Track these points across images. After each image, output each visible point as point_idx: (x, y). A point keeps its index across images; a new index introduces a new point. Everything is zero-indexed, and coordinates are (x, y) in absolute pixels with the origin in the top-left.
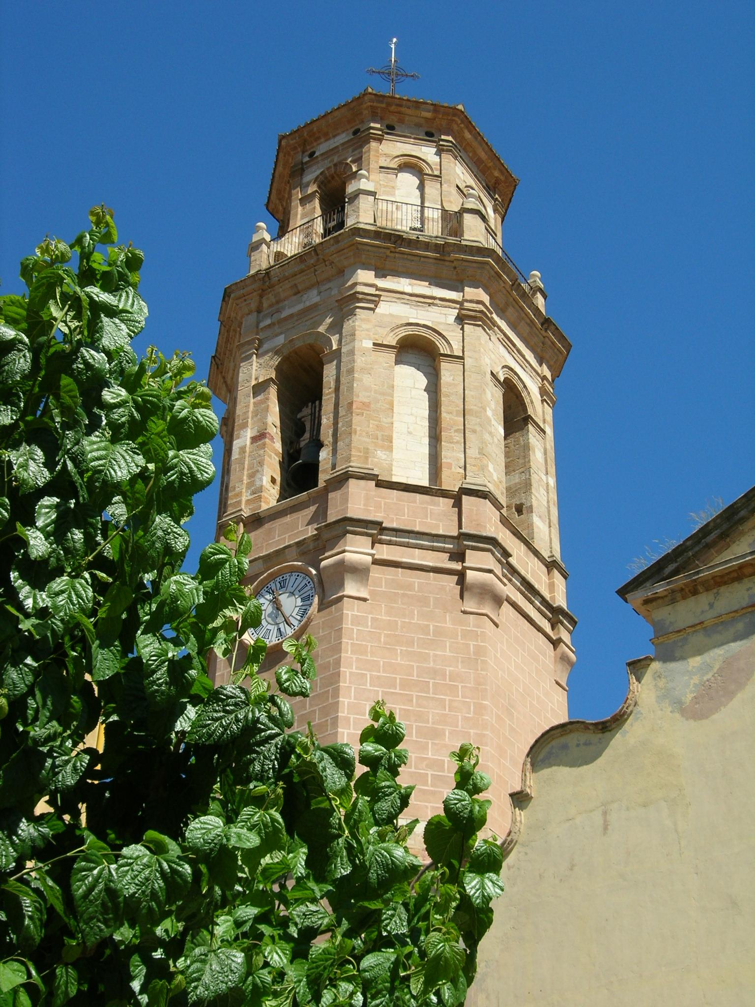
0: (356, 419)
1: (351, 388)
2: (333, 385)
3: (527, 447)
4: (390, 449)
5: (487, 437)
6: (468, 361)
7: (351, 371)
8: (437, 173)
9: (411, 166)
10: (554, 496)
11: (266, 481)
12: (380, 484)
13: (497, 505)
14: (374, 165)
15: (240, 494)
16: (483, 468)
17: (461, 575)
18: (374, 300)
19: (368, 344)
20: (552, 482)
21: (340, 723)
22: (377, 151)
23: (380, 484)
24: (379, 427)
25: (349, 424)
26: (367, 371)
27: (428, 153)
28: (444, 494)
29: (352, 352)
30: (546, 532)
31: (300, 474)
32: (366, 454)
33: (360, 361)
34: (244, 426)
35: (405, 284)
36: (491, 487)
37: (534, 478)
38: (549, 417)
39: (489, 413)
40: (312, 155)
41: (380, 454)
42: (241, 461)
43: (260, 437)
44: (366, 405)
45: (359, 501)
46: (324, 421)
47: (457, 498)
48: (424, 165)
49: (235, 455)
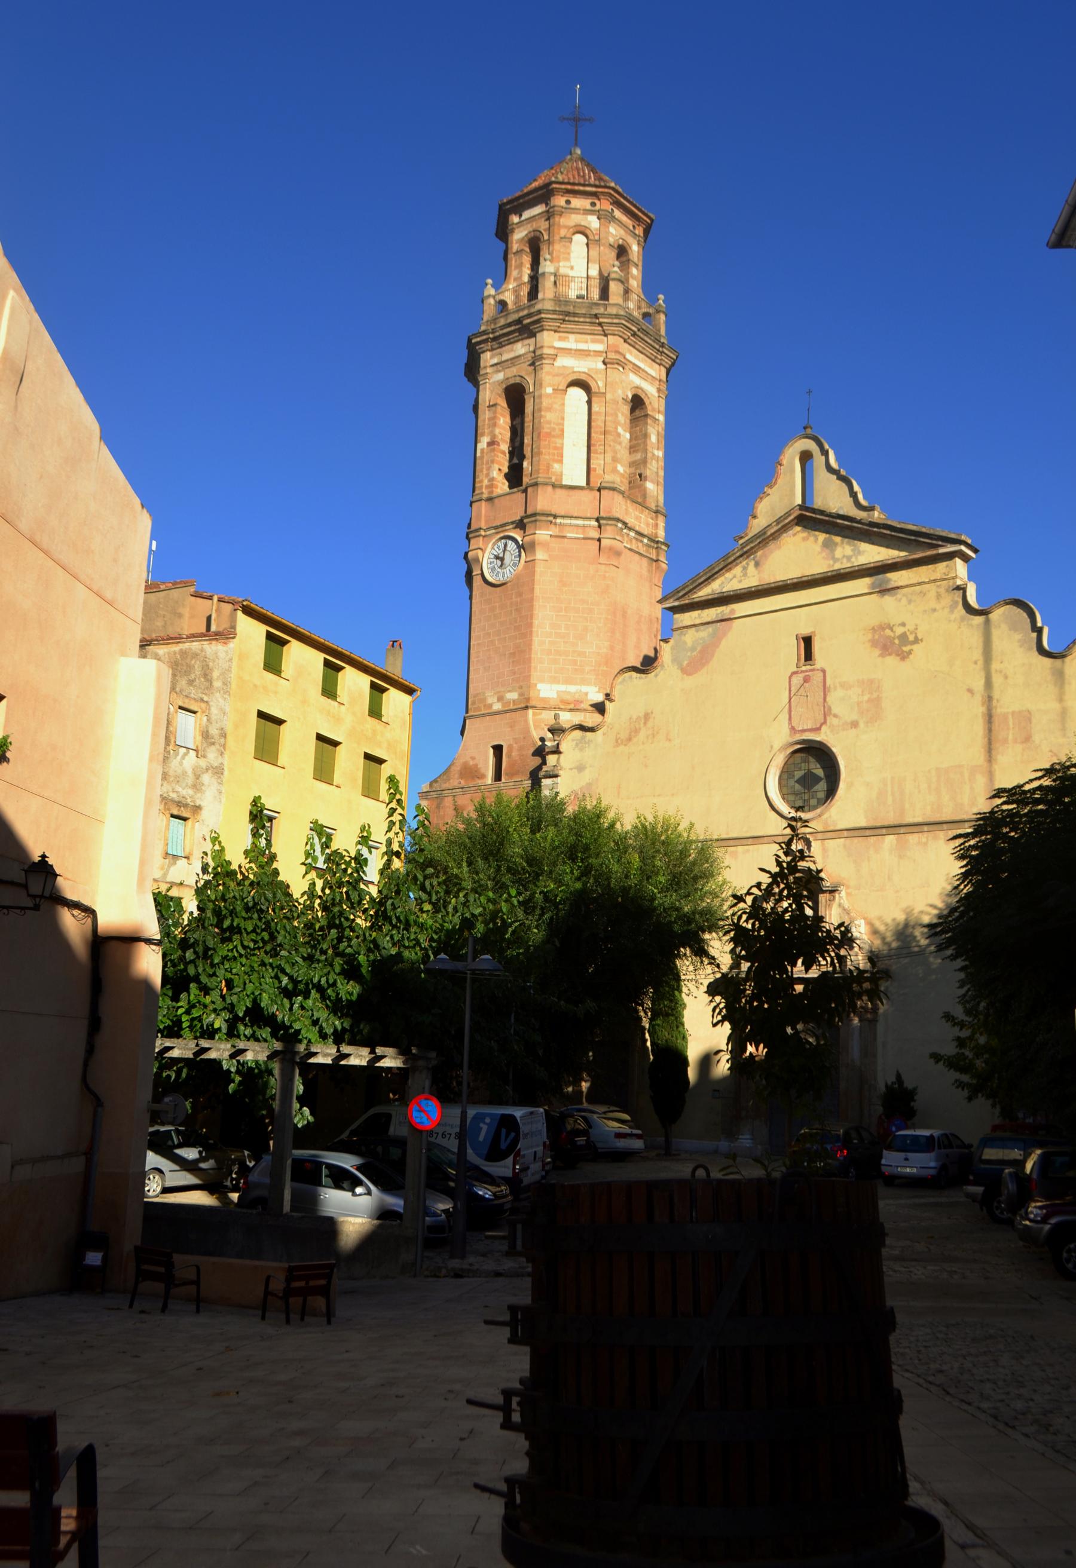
0: (543, 443)
1: (540, 422)
2: (531, 417)
3: (646, 436)
4: (561, 461)
5: (618, 447)
6: (609, 396)
7: (540, 410)
8: (597, 237)
9: (582, 231)
10: (662, 463)
11: (495, 474)
12: (554, 486)
13: (622, 493)
14: (557, 238)
15: (481, 481)
16: (615, 471)
17: (599, 540)
18: (555, 357)
19: (549, 390)
20: (660, 454)
21: (534, 634)
22: (559, 225)
23: (554, 486)
24: (556, 448)
25: (539, 447)
26: (549, 409)
27: (593, 222)
28: (592, 489)
29: (540, 397)
30: (654, 489)
31: (515, 476)
32: (549, 467)
33: (545, 402)
34: (483, 435)
35: (572, 342)
36: (618, 479)
37: (649, 455)
38: (662, 409)
39: (620, 430)
40: (521, 216)
41: (556, 466)
42: (482, 457)
43: (491, 444)
44: (549, 435)
45: (543, 500)
46: (526, 441)
47: (599, 490)
48: (588, 232)
49: (478, 454)
